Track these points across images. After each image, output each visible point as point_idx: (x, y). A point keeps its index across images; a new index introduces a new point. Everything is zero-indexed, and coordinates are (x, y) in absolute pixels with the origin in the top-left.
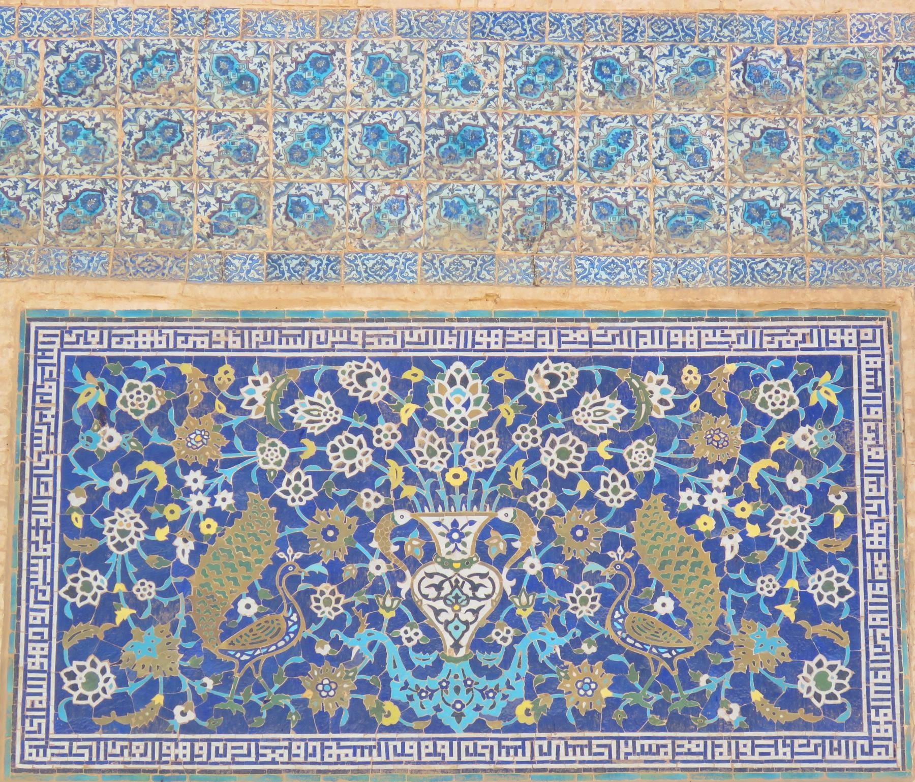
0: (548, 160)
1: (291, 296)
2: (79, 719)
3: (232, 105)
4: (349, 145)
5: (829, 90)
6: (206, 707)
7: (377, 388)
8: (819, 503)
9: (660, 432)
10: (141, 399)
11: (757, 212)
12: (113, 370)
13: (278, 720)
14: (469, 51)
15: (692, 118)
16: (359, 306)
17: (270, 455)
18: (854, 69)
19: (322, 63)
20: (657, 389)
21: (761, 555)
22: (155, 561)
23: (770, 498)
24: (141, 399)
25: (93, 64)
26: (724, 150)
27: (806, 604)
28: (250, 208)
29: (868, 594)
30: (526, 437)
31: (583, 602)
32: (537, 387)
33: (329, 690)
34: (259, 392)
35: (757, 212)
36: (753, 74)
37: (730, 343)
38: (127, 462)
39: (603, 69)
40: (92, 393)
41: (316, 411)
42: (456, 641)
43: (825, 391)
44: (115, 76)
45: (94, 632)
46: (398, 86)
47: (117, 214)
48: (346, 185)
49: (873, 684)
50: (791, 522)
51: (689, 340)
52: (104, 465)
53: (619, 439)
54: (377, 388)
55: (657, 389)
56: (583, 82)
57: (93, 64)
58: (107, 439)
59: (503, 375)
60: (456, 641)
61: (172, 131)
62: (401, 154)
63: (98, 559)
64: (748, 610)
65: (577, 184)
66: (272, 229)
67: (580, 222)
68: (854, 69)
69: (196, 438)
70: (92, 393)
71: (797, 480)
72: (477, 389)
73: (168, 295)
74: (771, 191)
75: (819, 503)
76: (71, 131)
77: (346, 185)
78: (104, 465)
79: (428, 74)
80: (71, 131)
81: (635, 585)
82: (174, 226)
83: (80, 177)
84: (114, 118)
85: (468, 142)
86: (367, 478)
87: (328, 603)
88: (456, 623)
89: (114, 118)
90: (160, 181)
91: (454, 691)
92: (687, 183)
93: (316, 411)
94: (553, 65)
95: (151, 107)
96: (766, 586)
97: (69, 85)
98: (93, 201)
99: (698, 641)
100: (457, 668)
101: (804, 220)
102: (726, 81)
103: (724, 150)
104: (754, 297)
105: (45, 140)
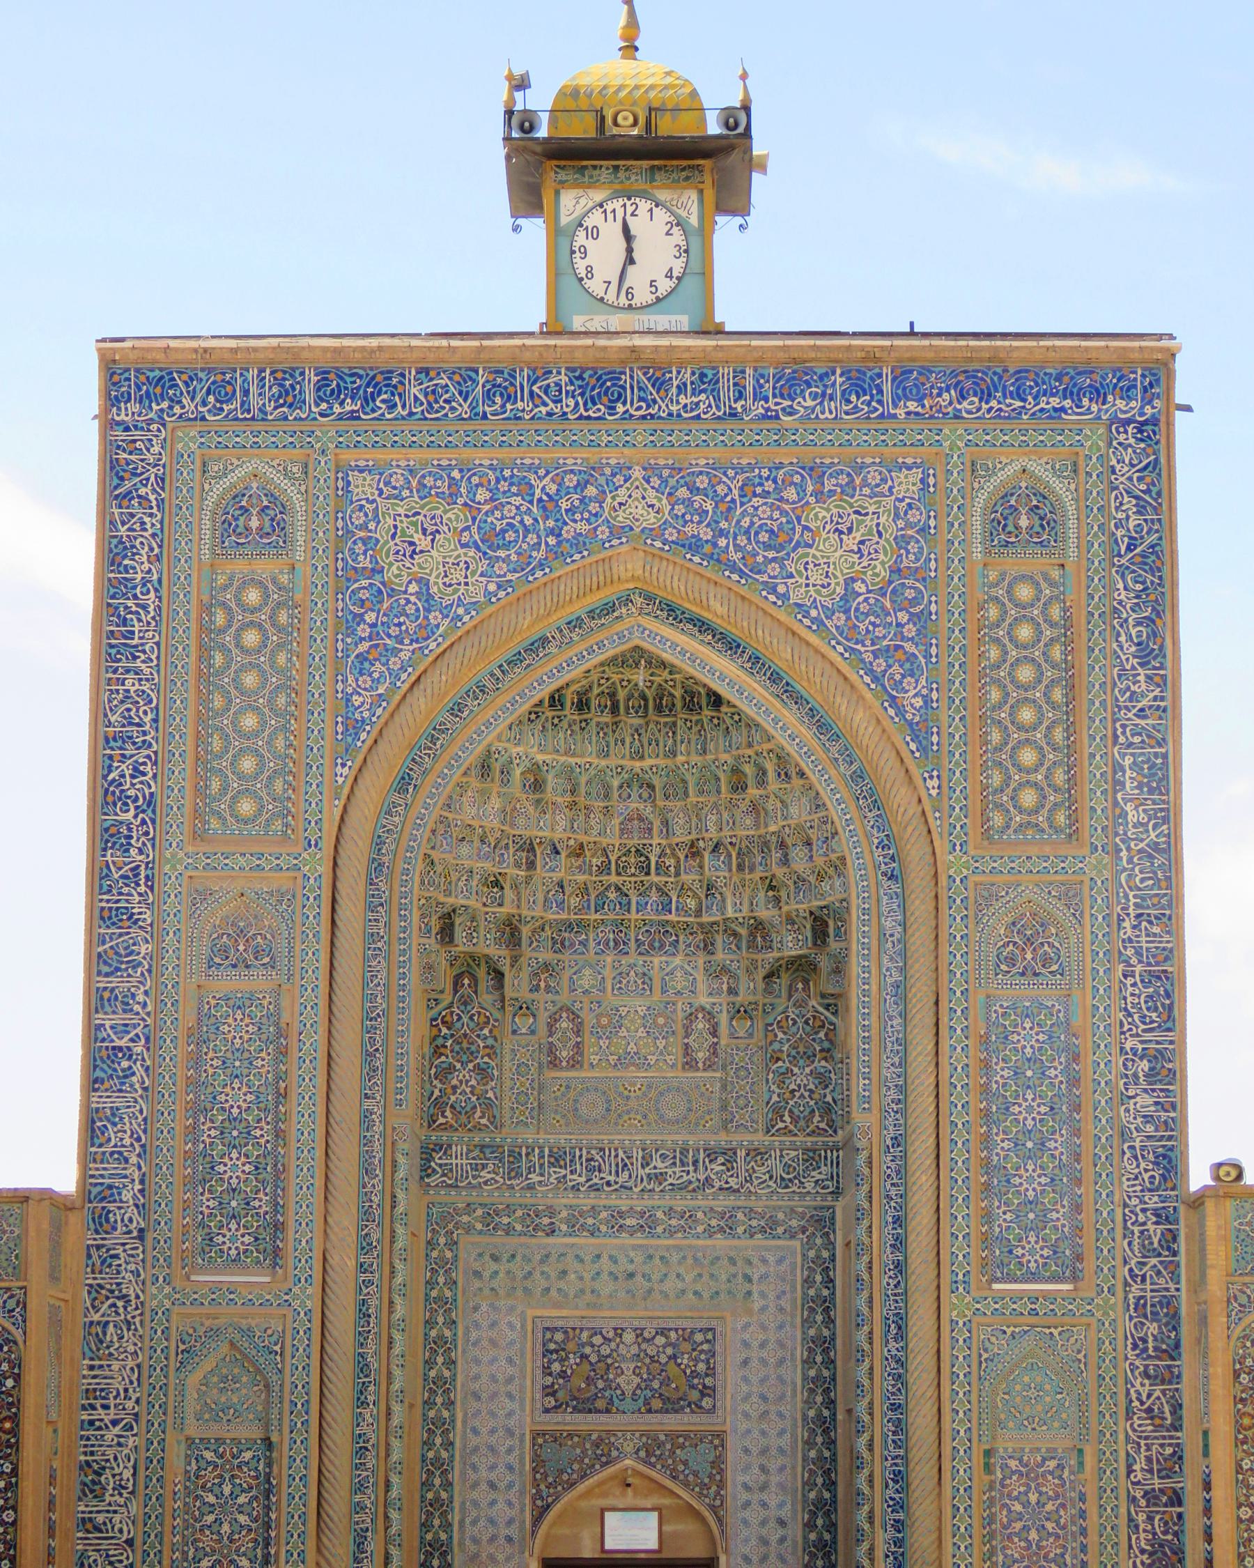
0: (649, 1280)
1: (593, 1314)
2: (547, 1411)
3: (578, 1266)
4: (605, 1276)
5: (712, 1263)
6: (574, 1408)
7: (611, 1335)
8: (708, 1362)
9: (674, 1346)
10: (559, 1337)
11: (696, 1293)
12: (554, 1330)
13: (590, 1411)
14: (632, 1254)
15: (682, 1271)
16: (606, 1318)
17: (588, 1350)
18: (718, 1258)
19: (598, 1256)
20: (673, 1334)
21: (695, 1374)
22: (562, 1374)
23: (696, 1360)
24: (559, 1337)
25: (547, 1256)
26: (689, 1278)
27: (704, 1386)
28: (582, 1291)
29: (718, 1384)
30: (644, 1346)
31: (656, 1385)
32: (646, 1334)
33: (600, 1404)
34: (585, 1335)
35: (696, 1293)
36: (695, 1259)
37: (688, 1324)
38: (556, 1351)
39: (662, 1258)
40: (548, 1335)
41: (597, 1340)
42: (629, 1393)
43: (710, 1336)
44: (552, 1259)
45: (549, 1391)
46: (616, 1262)
47: (553, 1293)
48: (606, 1287)
49: (718, 1404)
50: (701, 1367)
51: (680, 1323)
52: (551, 1352)
53: (664, 1347)
54: (611, 1335)
55: (673, 1334)
56: (657, 1261)
57: (547, 1256)
58: (552, 1346)
59: (639, 1332)
60: (629, 1393)
61: (564, 1272)
62: (616, 1278)
63: (550, 1374)
64: (693, 1387)
65: (656, 1286)
66: (588, 1297)
67: (656, 1295)
68: (718, 1258)
69: (571, 1346)
70: (548, 1335)
71: (703, 1357)
72: (633, 1335)
73: (564, 1313)
74: (699, 1287)
75: (708, 1362)
76: (543, 1273)
77: (606, 1287)
78: (551, 1352)
79: (622, 1260)
80: (543, 1273)
81: (666, 1382)
82: (566, 1296)
83: (545, 1284)
84: (551, 1269)
85: (631, 1275)
86: (609, 1356)
87: (600, 1384)
88: (629, 1389)
89: (551, 1269)
90: (562, 1285)
91: (628, 1404)
92: (680, 1285)
93: (597, 1340)
94: (650, 1257)
95: (560, 1267)
96: (696, 1381)
97: (542, 1262)
98: (548, 1290)
99: (680, 1394)
100: (628, 1400)
101: (706, 1295)
102: (690, 1261)
103: (689, 1278)
104: (696, 1314)
105: (537, 1275)
